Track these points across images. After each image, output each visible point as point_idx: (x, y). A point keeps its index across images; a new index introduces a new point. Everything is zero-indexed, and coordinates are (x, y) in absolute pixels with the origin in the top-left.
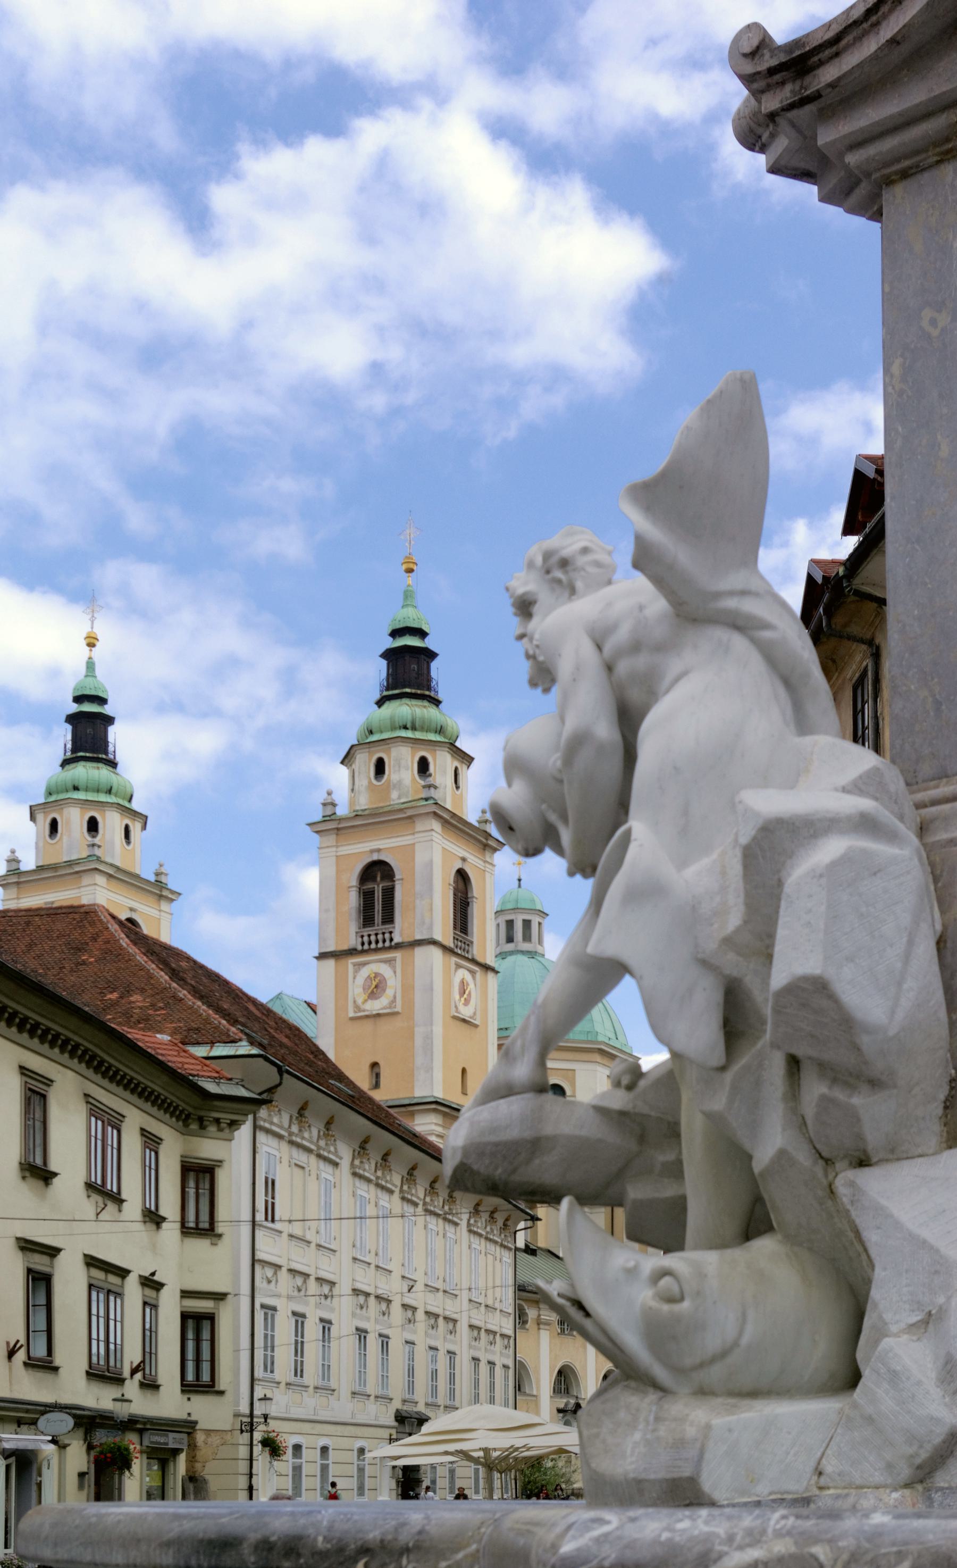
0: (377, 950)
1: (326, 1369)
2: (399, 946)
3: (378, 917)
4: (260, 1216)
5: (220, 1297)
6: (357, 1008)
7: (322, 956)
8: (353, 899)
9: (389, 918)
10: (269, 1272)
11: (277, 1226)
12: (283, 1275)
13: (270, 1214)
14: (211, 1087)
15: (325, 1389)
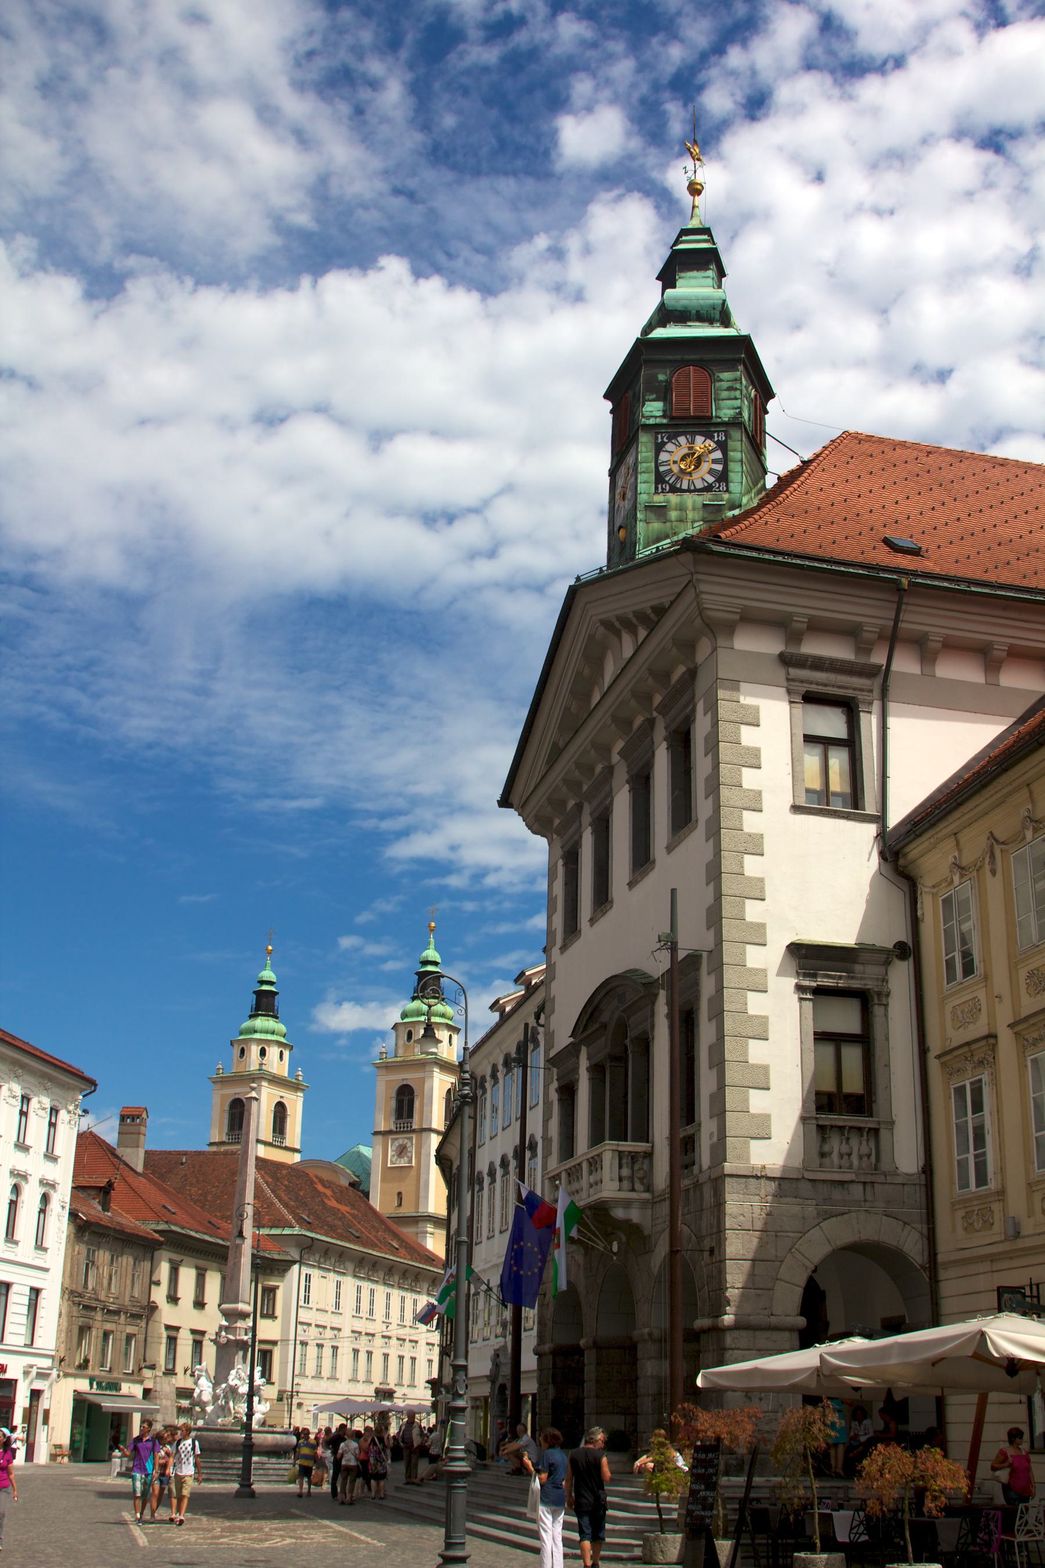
0: (403, 1132)
1: (334, 1368)
2: (414, 1131)
3: (405, 1114)
4: (301, 1303)
5: (274, 1343)
6: (392, 1163)
7: (376, 1133)
8: (393, 1104)
9: (410, 1115)
10: (305, 1327)
11: (310, 1305)
12: (313, 1328)
13: (307, 1299)
14: (276, 1257)
15: (333, 1378)
